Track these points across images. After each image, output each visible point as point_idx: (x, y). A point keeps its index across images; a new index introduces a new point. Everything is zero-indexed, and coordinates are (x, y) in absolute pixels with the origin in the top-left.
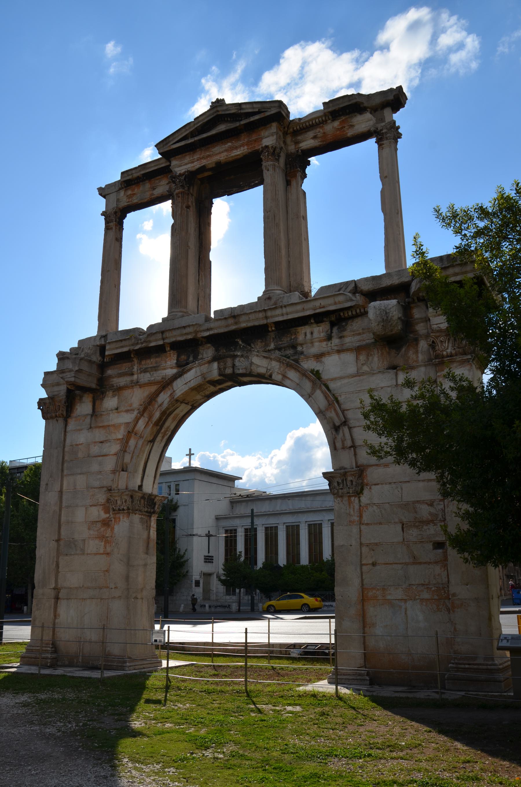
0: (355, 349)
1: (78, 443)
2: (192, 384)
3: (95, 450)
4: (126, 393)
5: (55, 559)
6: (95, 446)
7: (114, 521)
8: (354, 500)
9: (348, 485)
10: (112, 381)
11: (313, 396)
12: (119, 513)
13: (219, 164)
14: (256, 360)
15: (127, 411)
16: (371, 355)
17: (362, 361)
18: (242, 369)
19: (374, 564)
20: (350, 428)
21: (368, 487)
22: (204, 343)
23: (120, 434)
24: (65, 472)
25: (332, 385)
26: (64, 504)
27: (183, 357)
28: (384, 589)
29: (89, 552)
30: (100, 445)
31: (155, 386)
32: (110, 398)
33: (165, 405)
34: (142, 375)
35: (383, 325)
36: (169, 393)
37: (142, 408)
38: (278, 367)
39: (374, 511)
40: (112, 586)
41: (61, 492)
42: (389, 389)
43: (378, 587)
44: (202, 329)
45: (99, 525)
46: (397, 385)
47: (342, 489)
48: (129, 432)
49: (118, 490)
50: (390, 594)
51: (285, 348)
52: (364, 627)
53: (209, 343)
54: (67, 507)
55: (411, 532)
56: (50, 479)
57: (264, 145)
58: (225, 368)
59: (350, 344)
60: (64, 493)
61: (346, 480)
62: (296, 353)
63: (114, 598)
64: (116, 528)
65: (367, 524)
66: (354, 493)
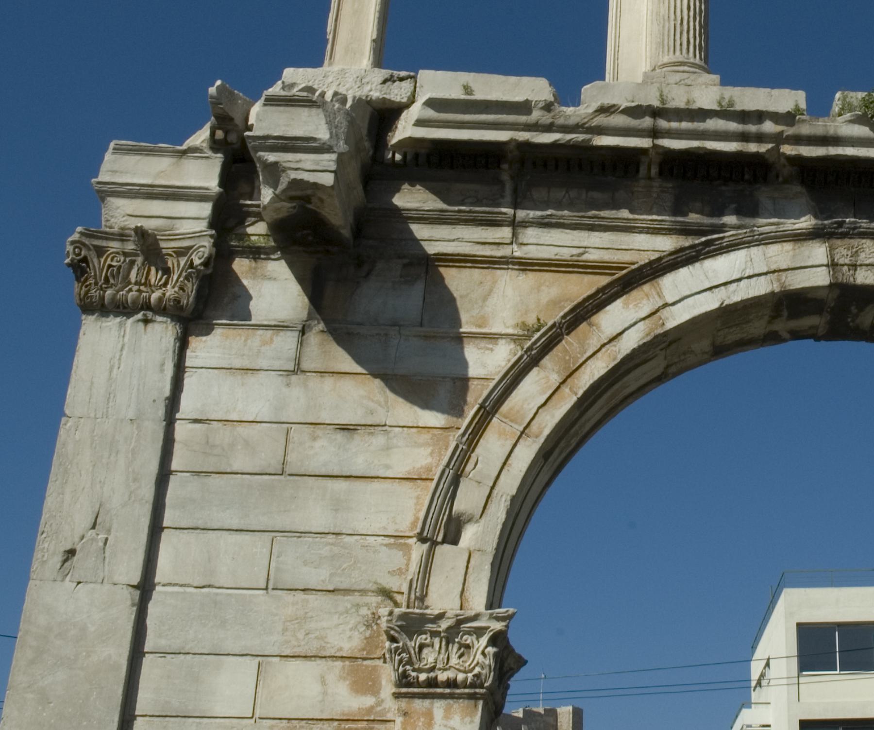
22: (781, 179)
31: (587, 278)
44: (805, 130)
53: (803, 183)
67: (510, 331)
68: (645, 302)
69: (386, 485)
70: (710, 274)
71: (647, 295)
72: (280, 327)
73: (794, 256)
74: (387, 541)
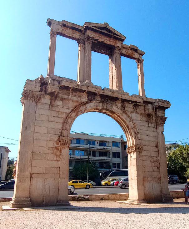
2: (93, 107)
4: (67, 101)
13: (102, 42)
23: (64, 116)
27: (90, 97)
29: (49, 159)
30: (54, 117)
34: (73, 97)
37: (74, 109)
40: (61, 173)
41: (34, 132)
45: (53, 149)
57: (118, 46)
58: (104, 106)
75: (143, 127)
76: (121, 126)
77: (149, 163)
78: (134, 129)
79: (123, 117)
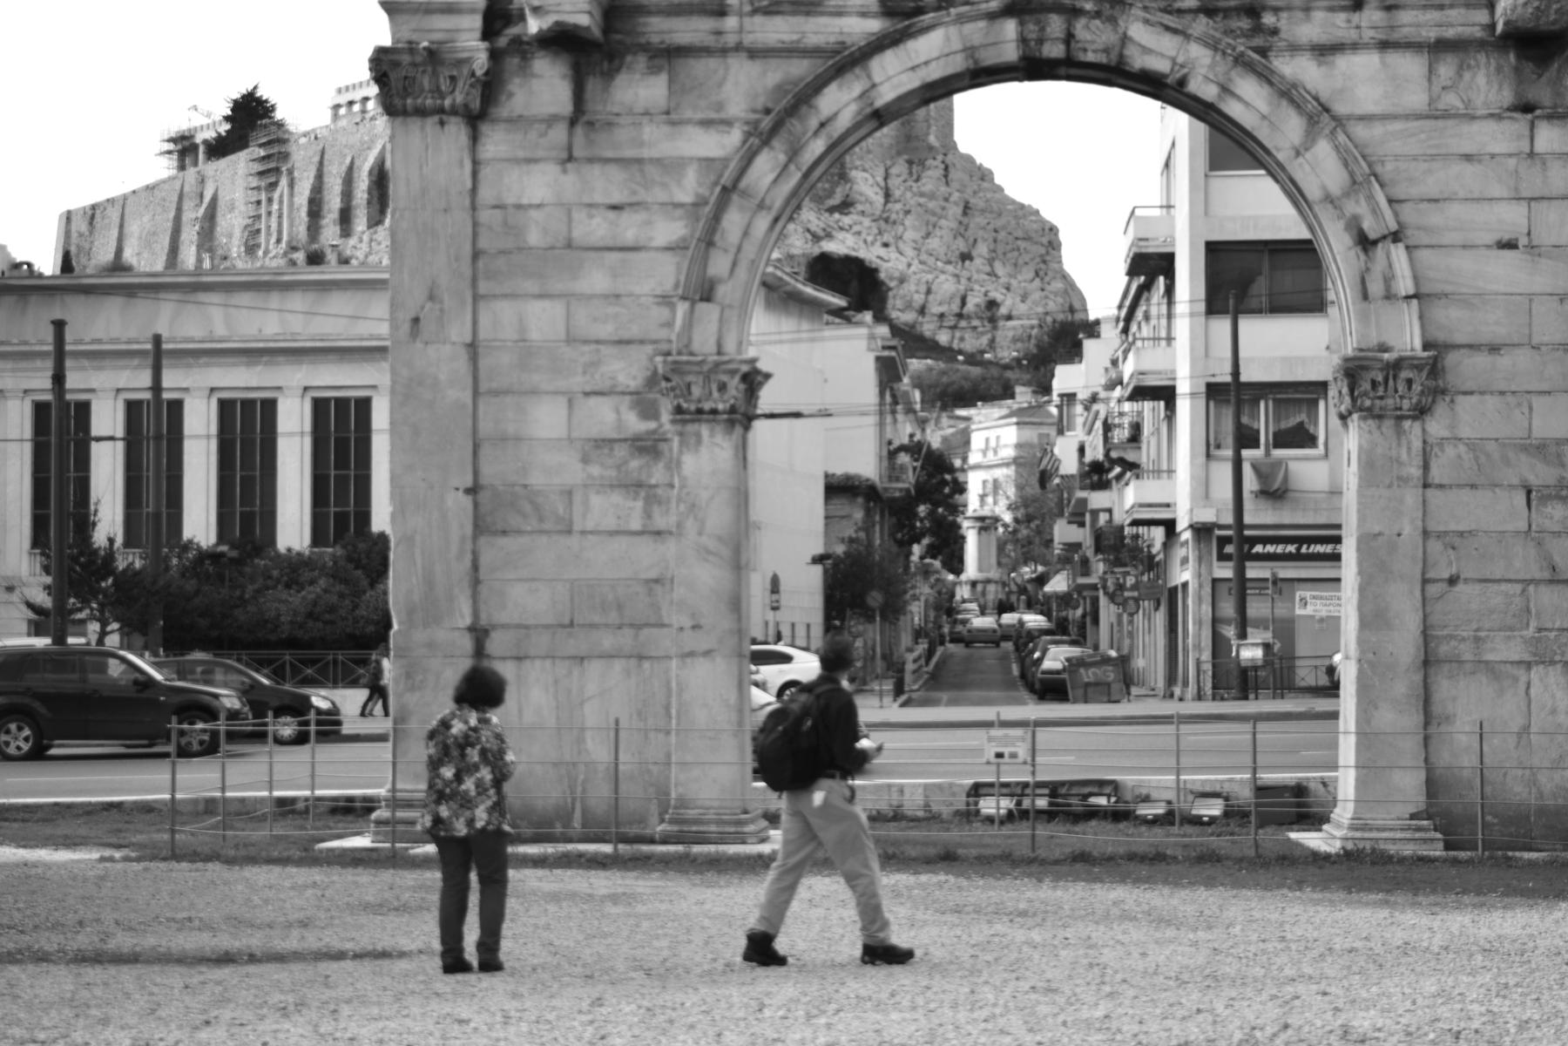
0: (1429, 47)
1: (525, 201)
2: (935, 73)
3: (595, 228)
4: (700, 67)
5: (469, 546)
6: (591, 217)
7: (682, 443)
8: (1411, 427)
9: (1400, 389)
10: (645, 24)
11: (1308, 155)
12: (699, 421)
14: (1139, 32)
15: (706, 123)
16: (1469, 67)
17: (1442, 78)
18: (1095, 51)
19: (1452, 581)
20: (1407, 247)
21: (1448, 399)
23: (688, 188)
24: (483, 287)
25: (1360, 131)
26: (483, 387)
28: (1477, 640)
29: (590, 526)
30: (612, 215)
32: (637, 76)
33: (845, 120)
34: (759, 20)
35: (1538, 8)
36: (857, 88)
37: (766, 123)
38: (1207, 61)
39: (1459, 457)
42: (1512, 162)
43: (1465, 634)
45: (621, 451)
46: (1532, 154)
47: (1381, 398)
48: (724, 189)
49: (692, 354)
50: (1493, 650)
51: (1227, 12)
52: (1427, 724)
54: (496, 393)
55: (1549, 509)
56: (429, 305)
58: (1041, 41)
59: (1412, 29)
60: (481, 350)
61: (1395, 377)
62: (1258, 29)
63: (691, 654)
64: (689, 463)
65: (1441, 486)
66: (1415, 410)
67: (743, 115)
68: (856, 83)
69: (652, 254)
70: (913, 55)
71: (858, 77)
72: (551, 120)
73: (987, 34)
74: (656, 300)
75: (1469, 169)
76: (1277, 181)
77: (1506, 510)
78: (1351, 207)
79: (1233, 109)
